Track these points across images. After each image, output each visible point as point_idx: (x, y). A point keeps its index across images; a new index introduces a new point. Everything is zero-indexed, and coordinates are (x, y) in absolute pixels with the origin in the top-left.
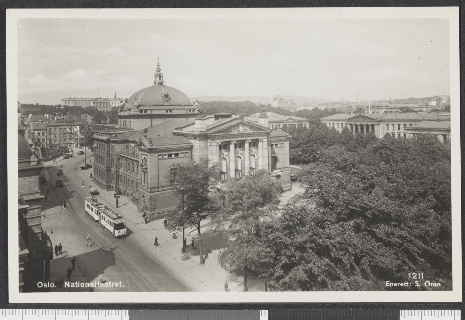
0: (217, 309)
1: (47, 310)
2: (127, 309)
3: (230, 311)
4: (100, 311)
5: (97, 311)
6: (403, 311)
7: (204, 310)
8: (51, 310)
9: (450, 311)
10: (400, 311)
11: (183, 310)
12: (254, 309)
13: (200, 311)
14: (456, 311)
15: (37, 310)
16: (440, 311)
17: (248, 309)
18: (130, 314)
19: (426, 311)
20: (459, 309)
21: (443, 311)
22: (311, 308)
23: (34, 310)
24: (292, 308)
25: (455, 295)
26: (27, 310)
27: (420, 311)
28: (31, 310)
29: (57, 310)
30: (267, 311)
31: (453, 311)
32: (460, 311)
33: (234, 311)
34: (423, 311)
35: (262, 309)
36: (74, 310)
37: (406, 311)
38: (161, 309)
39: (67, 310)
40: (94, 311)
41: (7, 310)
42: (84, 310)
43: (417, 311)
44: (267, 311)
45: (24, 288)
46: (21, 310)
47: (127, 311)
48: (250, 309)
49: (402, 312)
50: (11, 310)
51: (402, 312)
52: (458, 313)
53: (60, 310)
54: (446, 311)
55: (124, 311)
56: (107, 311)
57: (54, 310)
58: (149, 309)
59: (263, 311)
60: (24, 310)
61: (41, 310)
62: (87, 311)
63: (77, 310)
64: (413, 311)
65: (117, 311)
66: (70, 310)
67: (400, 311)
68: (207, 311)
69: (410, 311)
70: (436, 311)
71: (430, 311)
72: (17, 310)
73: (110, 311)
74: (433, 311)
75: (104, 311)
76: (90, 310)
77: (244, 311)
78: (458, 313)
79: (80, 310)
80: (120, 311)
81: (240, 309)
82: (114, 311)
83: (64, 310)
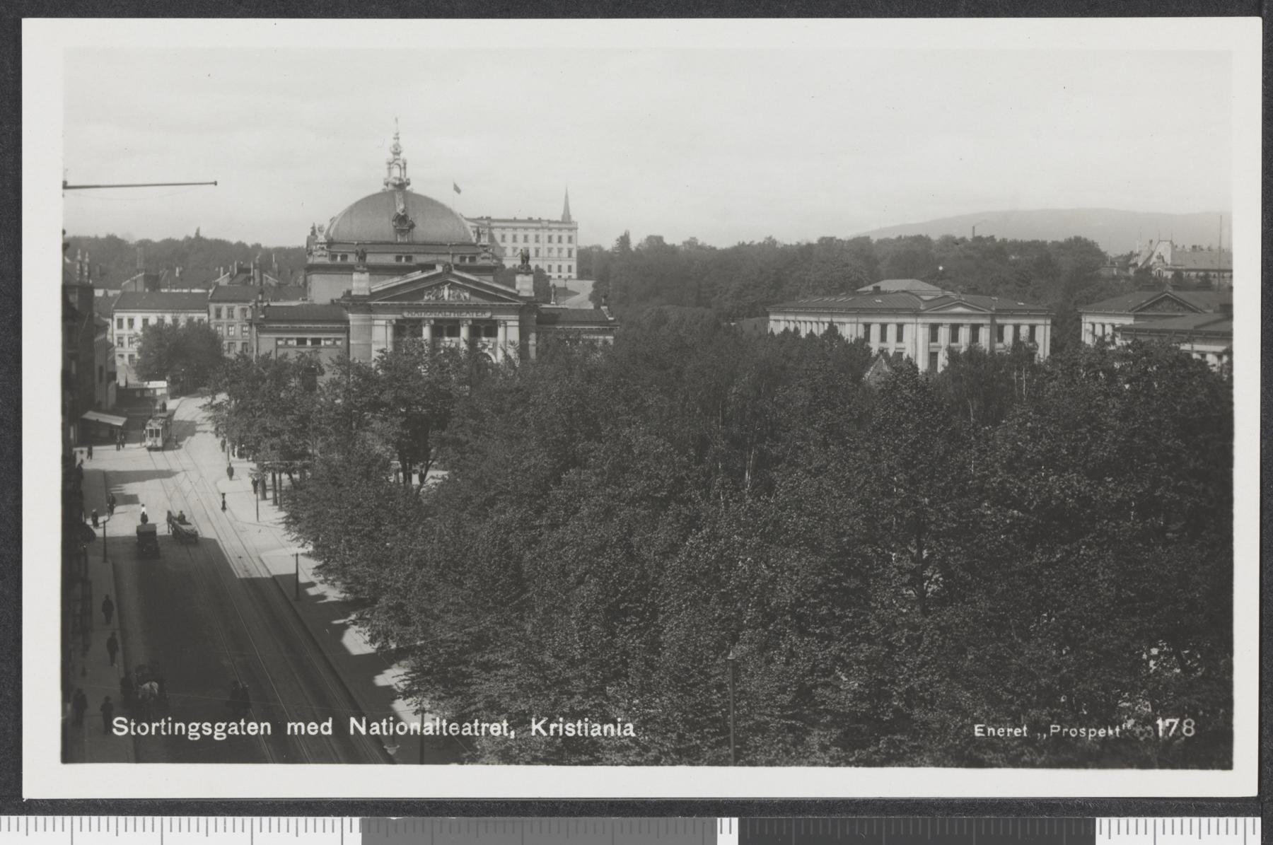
0: (600, 815)
1: (139, 819)
2: (356, 815)
3: (635, 820)
4: (283, 819)
5: (274, 819)
6: (1105, 820)
7: (565, 819)
8: (149, 819)
9: (1232, 820)
10: (1098, 819)
11: (508, 818)
13: (554, 819)
14: (1250, 820)
15: (113, 819)
16: (1204, 820)
17: (684, 815)
18: (365, 830)
19: (1168, 820)
20: (1255, 815)
21: (1214, 820)
22: (855, 812)
23: (104, 819)
24: (803, 812)
25: (1242, 779)
26: (85, 818)
27: (1150, 820)
28: (95, 819)
29: (167, 819)
30: (735, 821)
31: (1241, 820)
32: (1258, 820)
33: (645, 819)
34: (1159, 820)
36: (211, 819)
37: (1114, 820)
38: (448, 815)
39: (193, 819)
40: (265, 819)
41: (32, 818)
42: (238, 819)
43: (1141, 820)
44: (735, 821)
45: (72, 752)
46: (68, 819)
47: (356, 820)
48: (691, 815)
49: (1102, 823)
50: (41, 818)
51: (1102, 823)
52: (1253, 825)
53: (175, 819)
54: (1223, 820)
55: (347, 819)
56: (302, 819)
57: (158, 819)
58: (416, 815)
59: (726, 820)
60: (76, 819)
61: (121, 819)
62: (248, 819)
63: (220, 819)
64: (1132, 820)
65: (329, 819)
66: (202, 819)
67: (1098, 819)
69: (1123, 820)
70: (1195, 820)
71: (1177, 820)
72: (59, 818)
73: (311, 819)
74: (1186, 820)
75: (293, 819)
76: (256, 819)
78: (1253, 825)
79: (230, 819)
81: (662, 815)
82: (320, 819)
83: (184, 819)
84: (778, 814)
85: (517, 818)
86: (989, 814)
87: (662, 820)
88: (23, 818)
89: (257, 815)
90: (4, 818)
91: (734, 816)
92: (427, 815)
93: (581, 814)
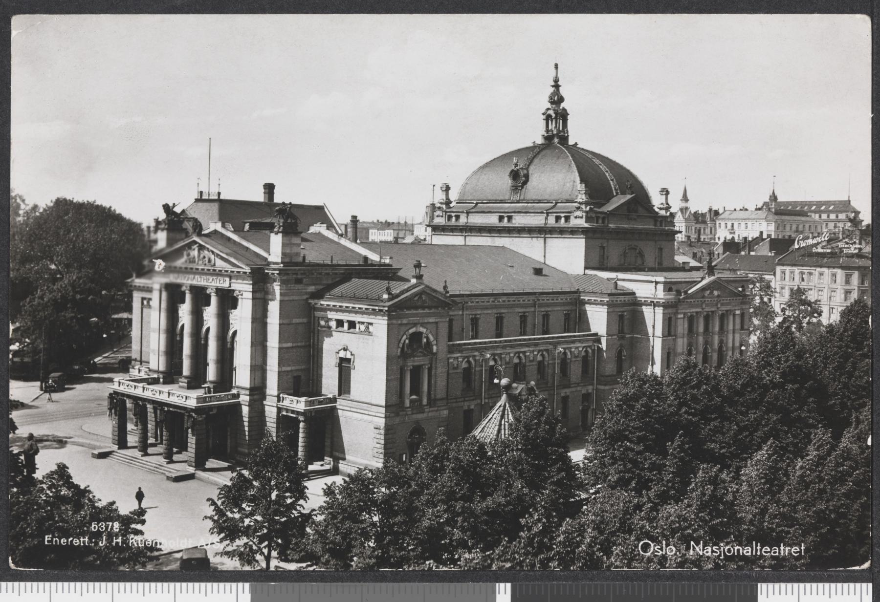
1: (97, 584)
2: (247, 581)
3: (440, 585)
4: (197, 584)
6: (764, 585)
7: (391, 584)
8: (103, 584)
9: (852, 585)
10: (759, 585)
12: (487, 581)
13: (384, 585)
14: (864, 585)
15: (78, 584)
18: (253, 592)
19: (808, 585)
20: (867, 581)
21: (839, 585)
22: (591, 580)
26: (60, 584)
27: (796, 585)
28: (66, 584)
29: (116, 584)
30: (509, 585)
31: (858, 585)
32: (870, 585)
33: (446, 585)
34: (802, 585)
35: (501, 582)
36: (147, 584)
37: (771, 585)
39: (134, 584)
40: (184, 584)
42: (166, 584)
43: (789, 585)
44: (509, 585)
46: (47, 584)
50: (29, 584)
53: (122, 584)
54: (846, 585)
55: (240, 584)
56: (209, 585)
57: (110, 584)
59: (502, 585)
60: (53, 584)
61: (85, 584)
62: (172, 584)
63: (153, 584)
64: (783, 585)
65: (228, 585)
66: (141, 584)
68: (396, 584)
69: (777, 585)
70: (827, 585)
71: (814, 585)
72: (41, 584)
73: (215, 585)
75: (203, 584)
76: (178, 584)
77: (465, 585)
79: (159, 584)
80: (234, 585)
81: (458, 582)
82: (222, 585)
83: (128, 584)
84: (538, 580)
85: (358, 584)
86: (684, 580)
87: (458, 585)
88: (16, 584)
89: (178, 581)
90: (3, 584)
91: (508, 582)
92: (296, 581)
93: (402, 581)
